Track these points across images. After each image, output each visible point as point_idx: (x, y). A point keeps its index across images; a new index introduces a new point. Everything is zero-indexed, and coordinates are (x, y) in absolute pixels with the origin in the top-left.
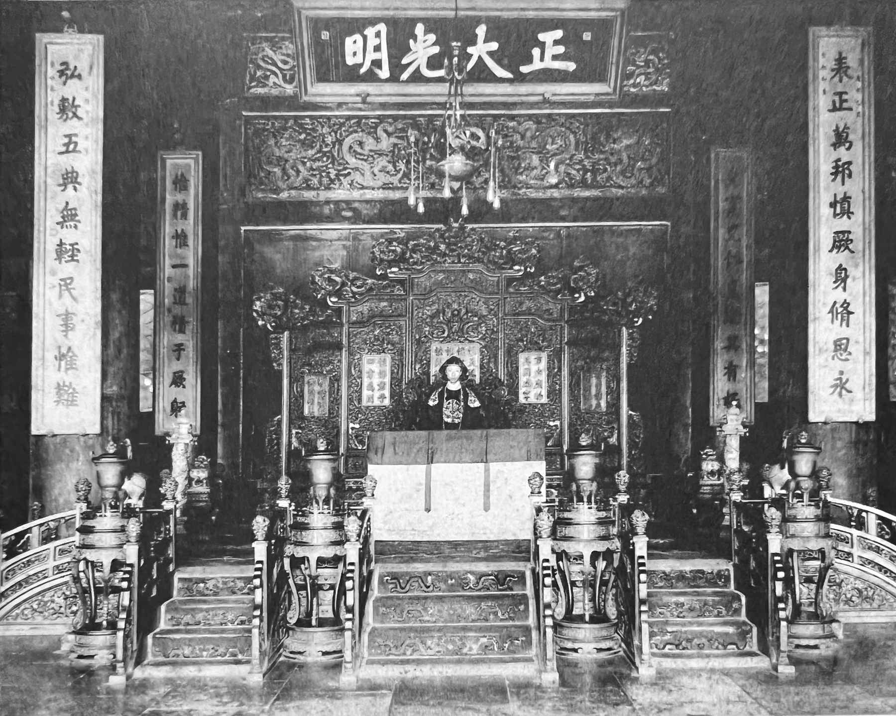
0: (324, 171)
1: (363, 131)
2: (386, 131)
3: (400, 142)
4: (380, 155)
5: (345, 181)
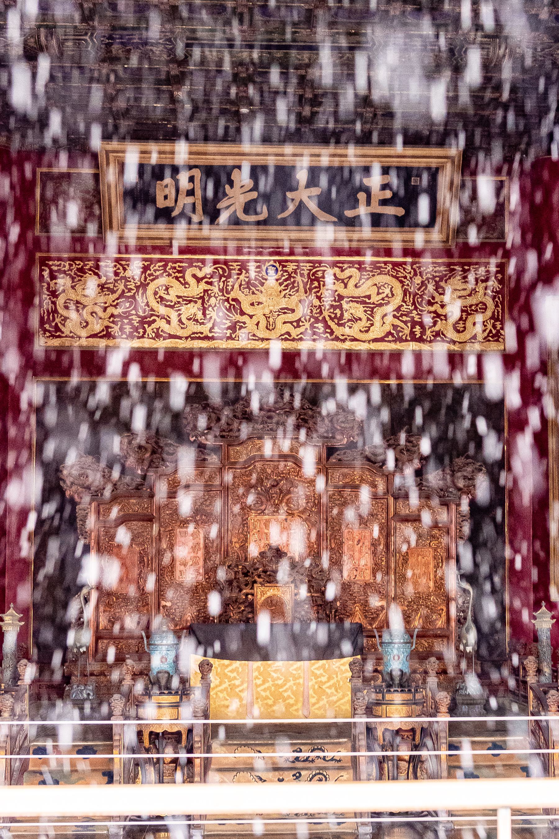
0: (127, 318)
1: (169, 275)
2: (194, 276)
3: (208, 287)
4: (190, 301)
5: (149, 330)
